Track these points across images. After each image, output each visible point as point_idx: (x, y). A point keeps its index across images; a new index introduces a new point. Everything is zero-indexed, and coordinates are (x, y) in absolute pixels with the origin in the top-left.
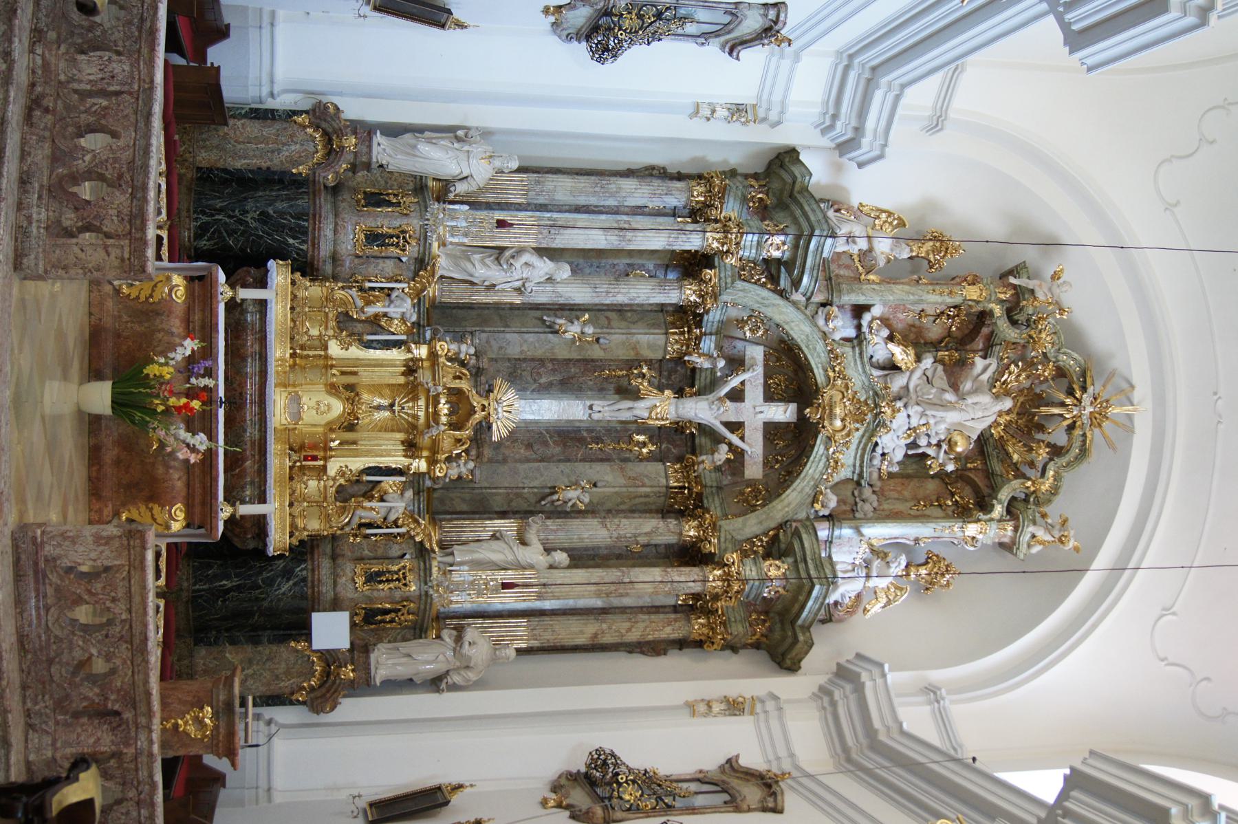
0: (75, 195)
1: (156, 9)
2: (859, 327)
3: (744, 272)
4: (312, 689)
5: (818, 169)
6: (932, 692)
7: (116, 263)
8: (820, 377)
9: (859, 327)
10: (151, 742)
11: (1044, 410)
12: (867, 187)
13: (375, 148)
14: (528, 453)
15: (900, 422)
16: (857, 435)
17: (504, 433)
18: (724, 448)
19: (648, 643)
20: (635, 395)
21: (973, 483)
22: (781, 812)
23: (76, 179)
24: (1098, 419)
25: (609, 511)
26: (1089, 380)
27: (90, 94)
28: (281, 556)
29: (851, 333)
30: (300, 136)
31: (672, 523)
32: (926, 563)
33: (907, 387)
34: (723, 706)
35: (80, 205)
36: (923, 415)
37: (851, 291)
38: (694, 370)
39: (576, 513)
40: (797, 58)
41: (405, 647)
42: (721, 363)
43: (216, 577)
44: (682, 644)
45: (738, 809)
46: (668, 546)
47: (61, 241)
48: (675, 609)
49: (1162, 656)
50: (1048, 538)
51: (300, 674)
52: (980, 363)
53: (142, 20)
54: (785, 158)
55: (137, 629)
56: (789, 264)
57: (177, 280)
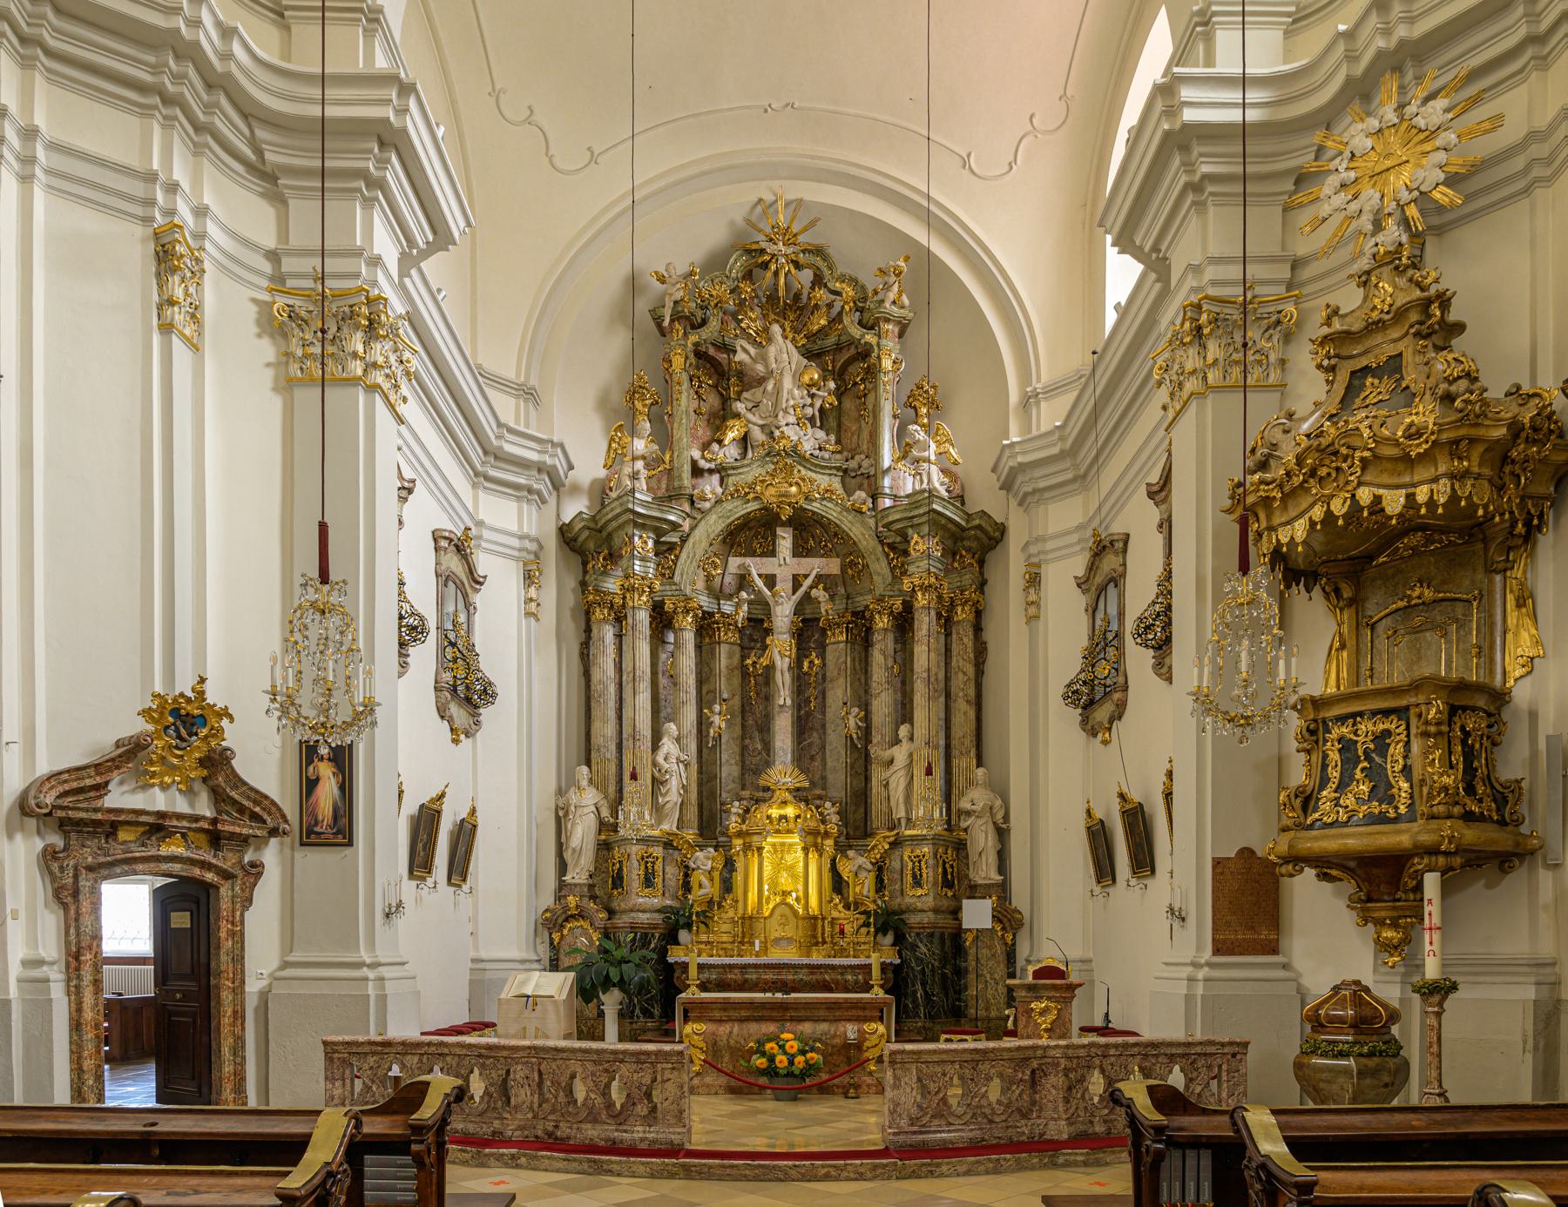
0: (622, 1106)
1: (470, 1046)
2: (711, 471)
3: (667, 574)
4: (1003, 929)
5: (575, 508)
6: (1029, 401)
7: (676, 1073)
8: (753, 506)
9: (711, 471)
10: (1057, 1046)
11: (781, 293)
12: (589, 465)
13: (576, 881)
14: (818, 758)
15: (792, 433)
16: (804, 472)
17: (802, 777)
18: (814, 592)
19: (976, 657)
20: (770, 668)
21: (845, 366)
22: (1128, 535)
23: (610, 1105)
24: (789, 237)
25: (866, 692)
26: (754, 247)
27: (541, 1094)
28: (899, 953)
29: (716, 478)
30: (569, 939)
31: (877, 637)
32: (915, 408)
33: (762, 427)
34: (1032, 591)
35: (630, 1101)
36: (786, 411)
37: (680, 478)
38: (749, 620)
39: (867, 718)
40: (480, 524)
41: (973, 857)
42: (744, 595)
43: (915, 1001)
44: (978, 629)
45: (1123, 575)
46: (896, 642)
47: (660, 1116)
48: (948, 635)
49: (1007, 168)
50: (896, 288)
51: (992, 939)
52: (741, 356)
53: (480, 1056)
54: (566, 535)
55: (967, 1057)
56: (659, 533)
57: (688, 1029)
